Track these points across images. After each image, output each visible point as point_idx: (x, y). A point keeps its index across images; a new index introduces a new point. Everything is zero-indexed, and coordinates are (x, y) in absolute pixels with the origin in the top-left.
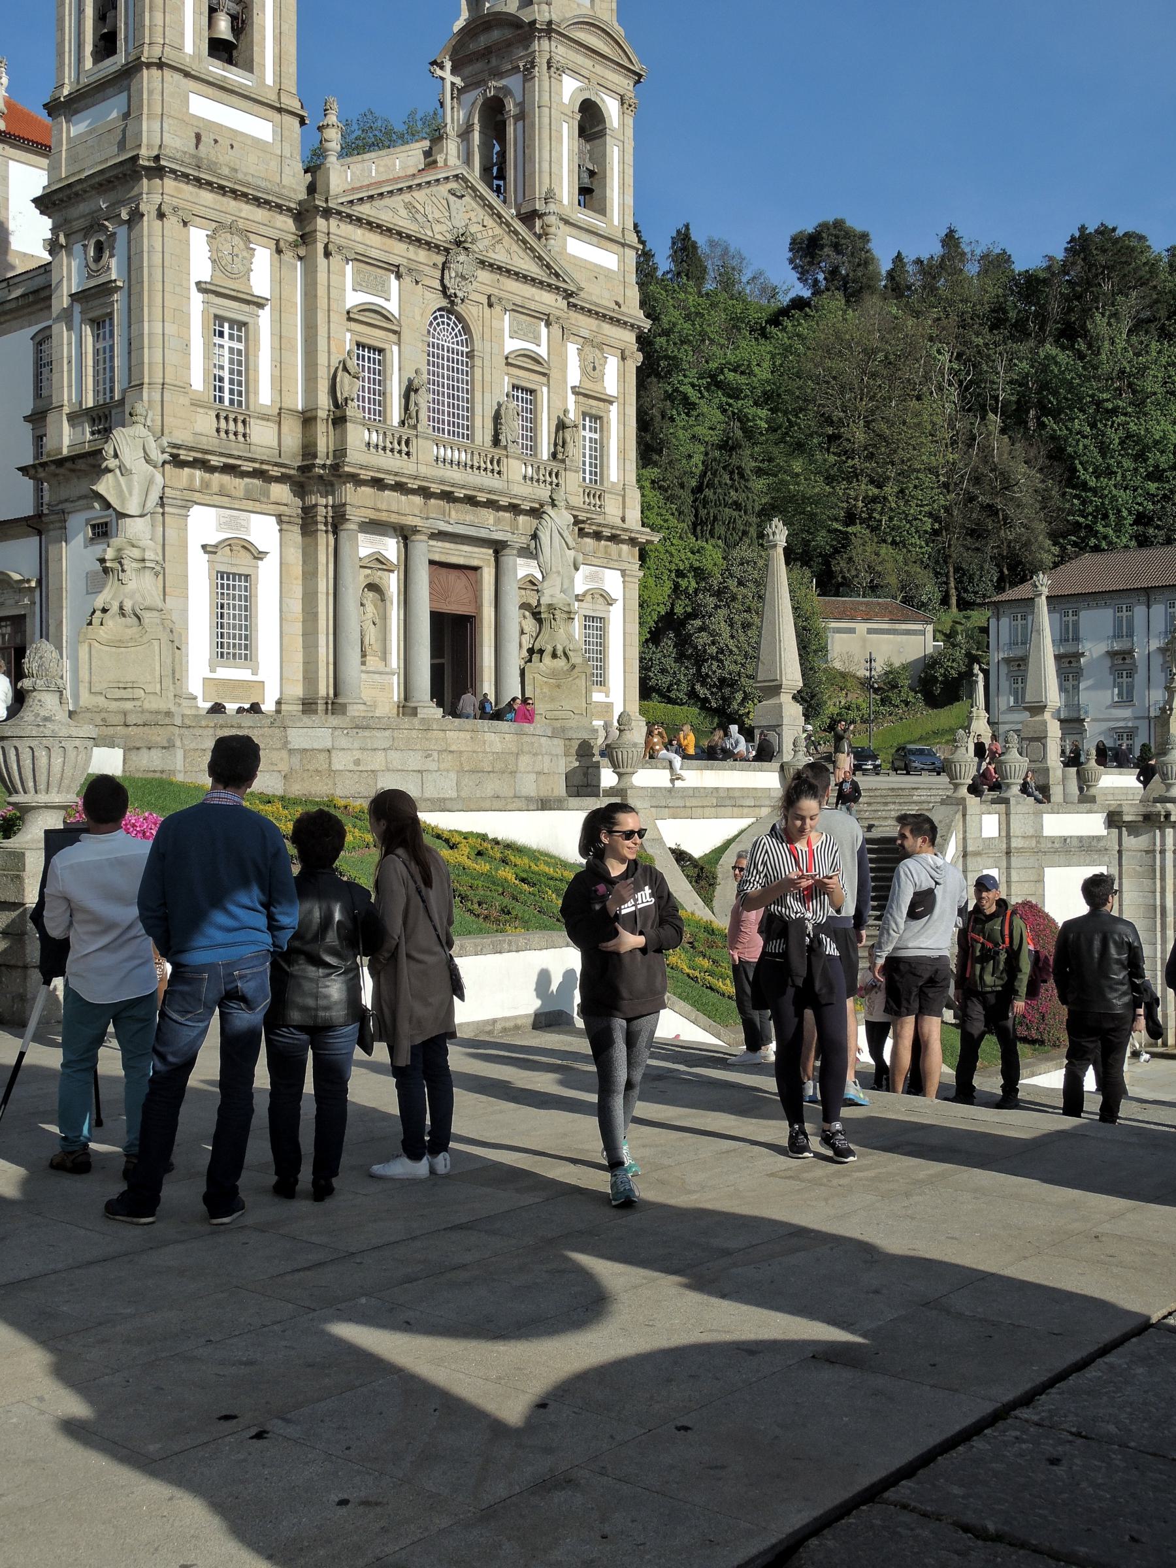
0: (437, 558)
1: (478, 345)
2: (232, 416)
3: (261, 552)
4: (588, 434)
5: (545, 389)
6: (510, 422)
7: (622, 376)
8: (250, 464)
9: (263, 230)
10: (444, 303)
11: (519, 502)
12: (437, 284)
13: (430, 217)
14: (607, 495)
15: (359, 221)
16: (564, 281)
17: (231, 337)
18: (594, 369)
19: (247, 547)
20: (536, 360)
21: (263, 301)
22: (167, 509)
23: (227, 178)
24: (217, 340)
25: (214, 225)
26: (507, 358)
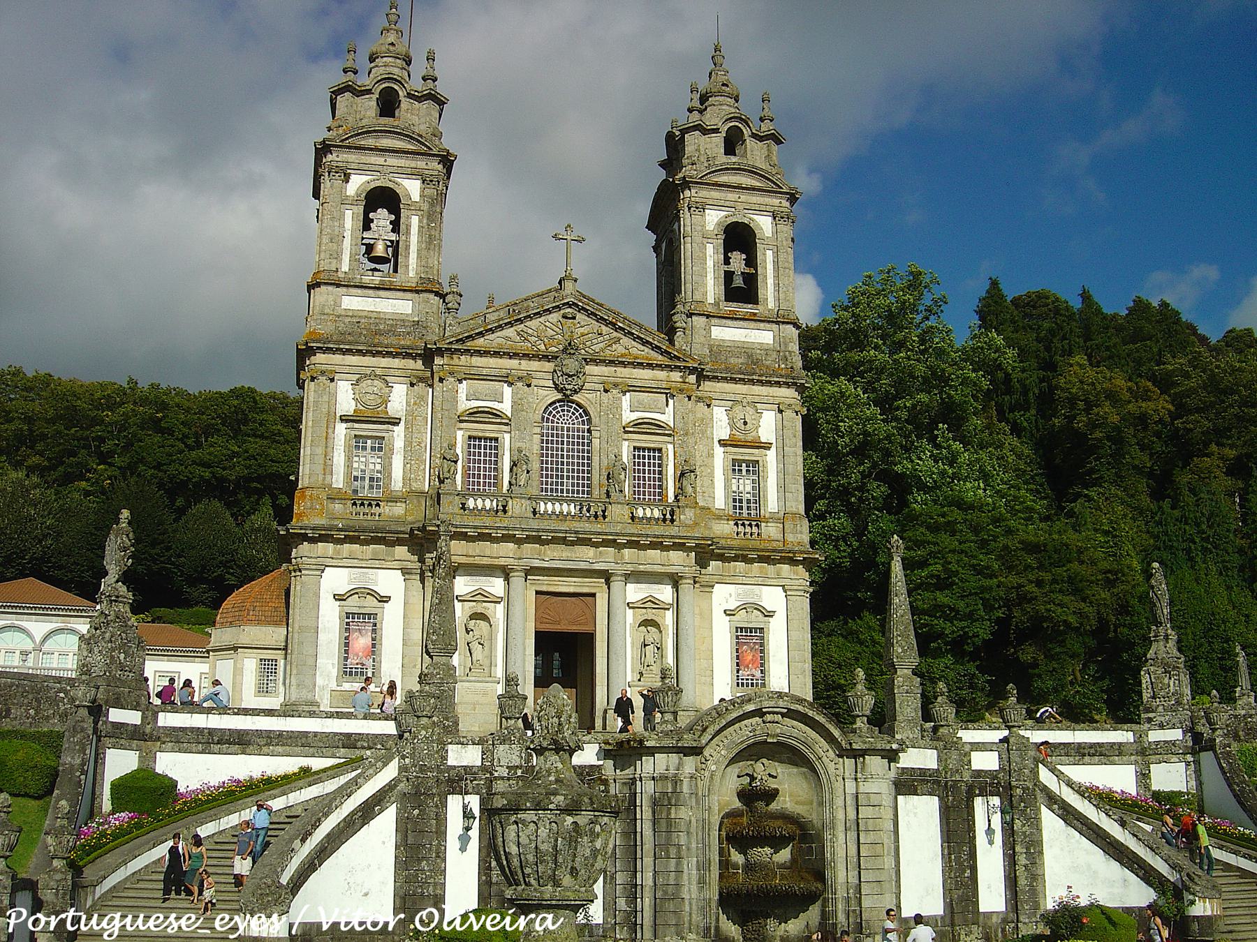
0: (544, 589)
1: (595, 420)
5: (670, 447)
7: (781, 428)
10: (560, 396)
12: (550, 384)
16: (684, 361)
18: (745, 423)
19: (372, 593)
21: (398, 421)
22: (303, 572)
25: (358, 376)
26: (624, 428)
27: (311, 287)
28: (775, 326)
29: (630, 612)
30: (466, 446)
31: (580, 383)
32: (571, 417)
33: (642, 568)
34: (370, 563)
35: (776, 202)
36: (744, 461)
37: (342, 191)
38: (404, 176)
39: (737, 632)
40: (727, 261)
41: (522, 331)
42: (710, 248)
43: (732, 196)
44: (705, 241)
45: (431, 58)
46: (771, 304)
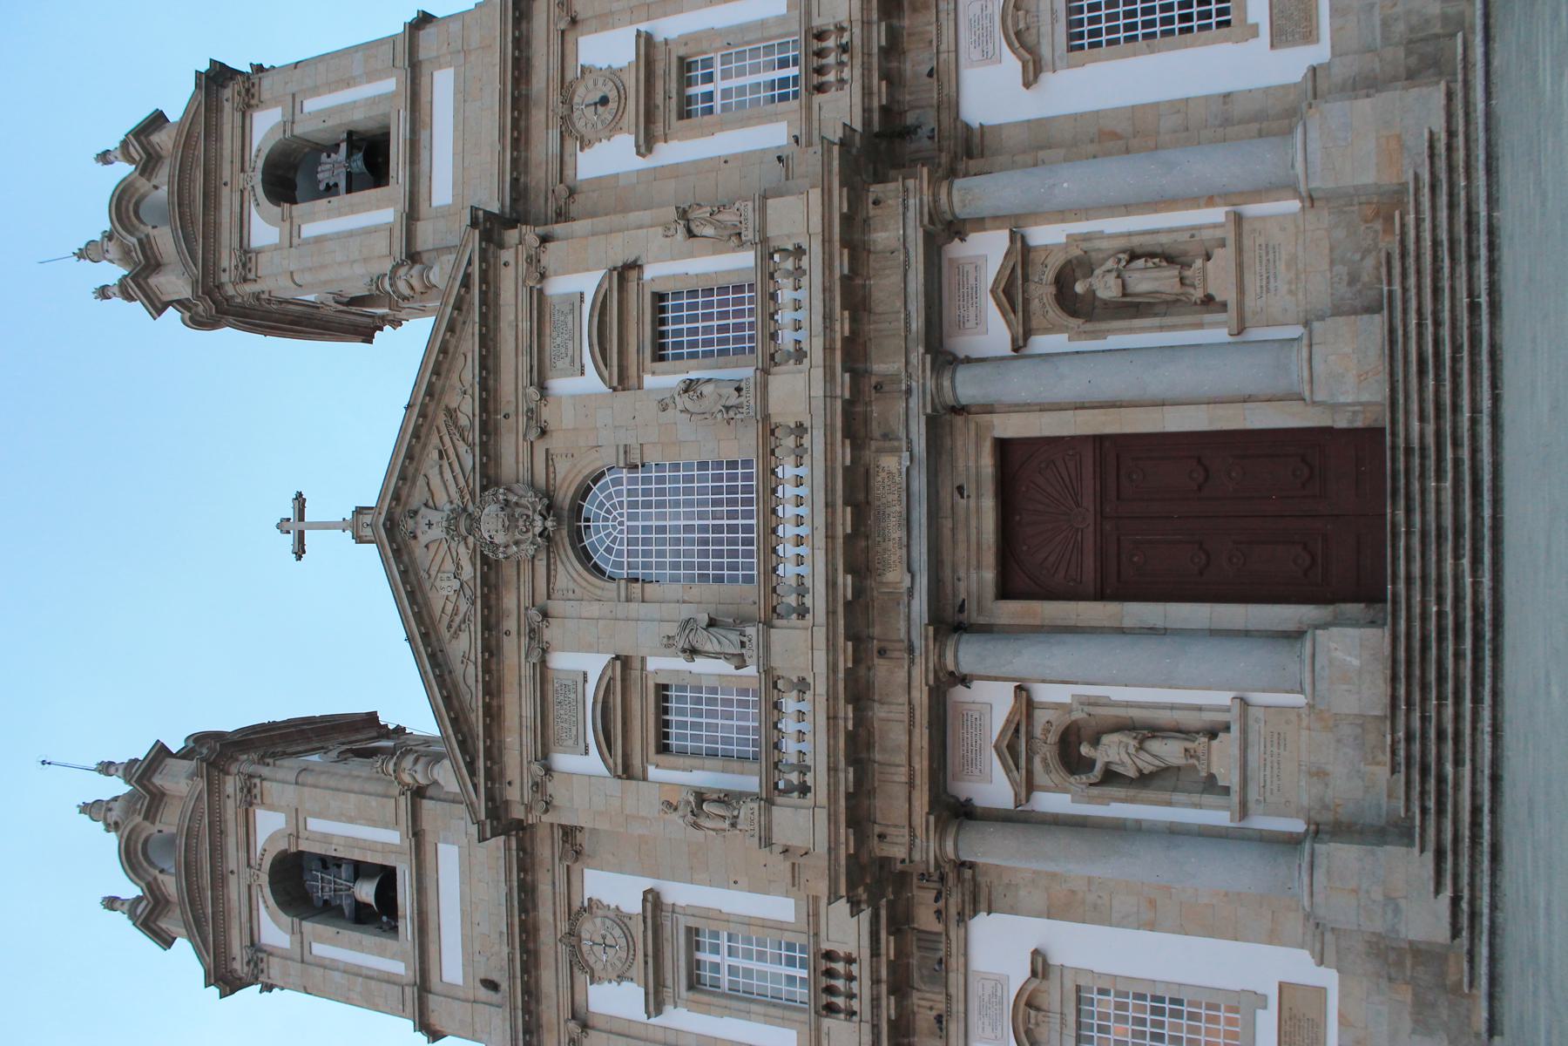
0: (989, 575)
1: (606, 457)
2: (824, 981)
3: (1034, 973)
4: (718, 86)
6: (706, 404)
7: (605, 21)
8: (884, 1003)
9: (561, 887)
11: (839, 405)
13: (456, 584)
14: (817, 22)
15: (494, 755)
16: (469, 263)
17: (715, 949)
18: (604, 101)
19: (1029, 1003)
20: (601, 309)
21: (650, 897)
23: (511, 960)
24: (725, 979)
25: (576, 970)
27: (435, 1035)
28: (425, 69)
29: (1043, 343)
30: (681, 761)
31: (529, 498)
32: (608, 511)
33: (917, 324)
34: (956, 988)
35: (227, 107)
36: (680, 92)
37: (285, 956)
38: (252, 839)
39: (1081, 47)
40: (331, 190)
41: (449, 626)
42: (309, 230)
43: (228, 199)
44: (296, 241)
45: (106, 768)
46: (389, 85)
